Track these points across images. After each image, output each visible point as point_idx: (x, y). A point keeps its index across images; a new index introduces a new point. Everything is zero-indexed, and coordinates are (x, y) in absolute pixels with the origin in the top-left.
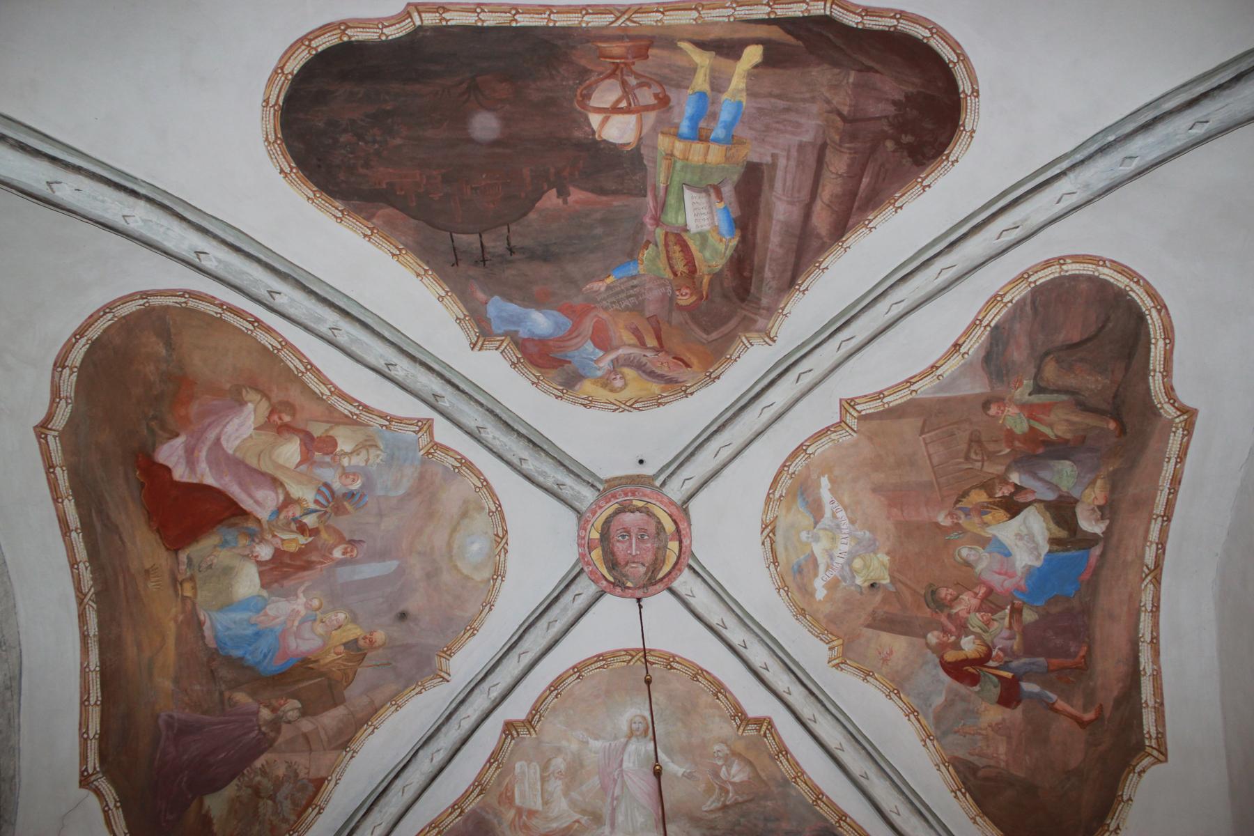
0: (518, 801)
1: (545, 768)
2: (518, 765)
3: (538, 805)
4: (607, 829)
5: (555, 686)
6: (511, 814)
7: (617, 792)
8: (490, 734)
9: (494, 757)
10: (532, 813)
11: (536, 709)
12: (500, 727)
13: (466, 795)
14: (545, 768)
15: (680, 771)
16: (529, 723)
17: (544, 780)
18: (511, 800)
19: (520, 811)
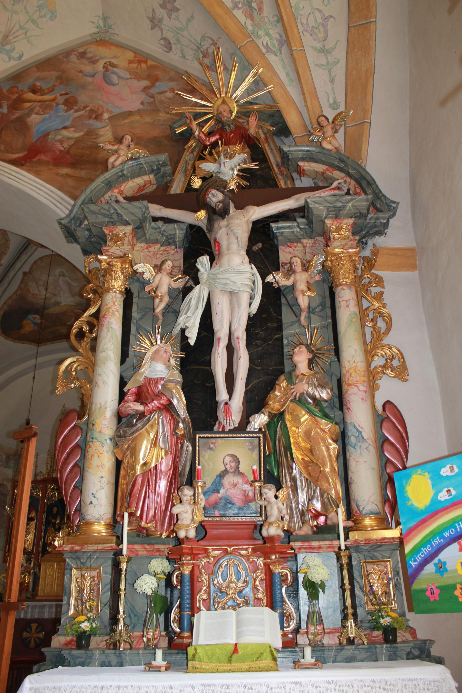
0: (31, 292)
1: (37, 284)
2: (29, 283)
3: (37, 292)
4: (59, 297)
5: (35, 262)
6: (31, 295)
7: (59, 289)
8: (20, 276)
9: (22, 281)
10: (37, 295)
11: (31, 268)
12: (22, 273)
13: (17, 291)
14: (37, 284)
15: (76, 285)
16: (30, 272)
17: (37, 287)
18: (29, 292)
19: (33, 294)
